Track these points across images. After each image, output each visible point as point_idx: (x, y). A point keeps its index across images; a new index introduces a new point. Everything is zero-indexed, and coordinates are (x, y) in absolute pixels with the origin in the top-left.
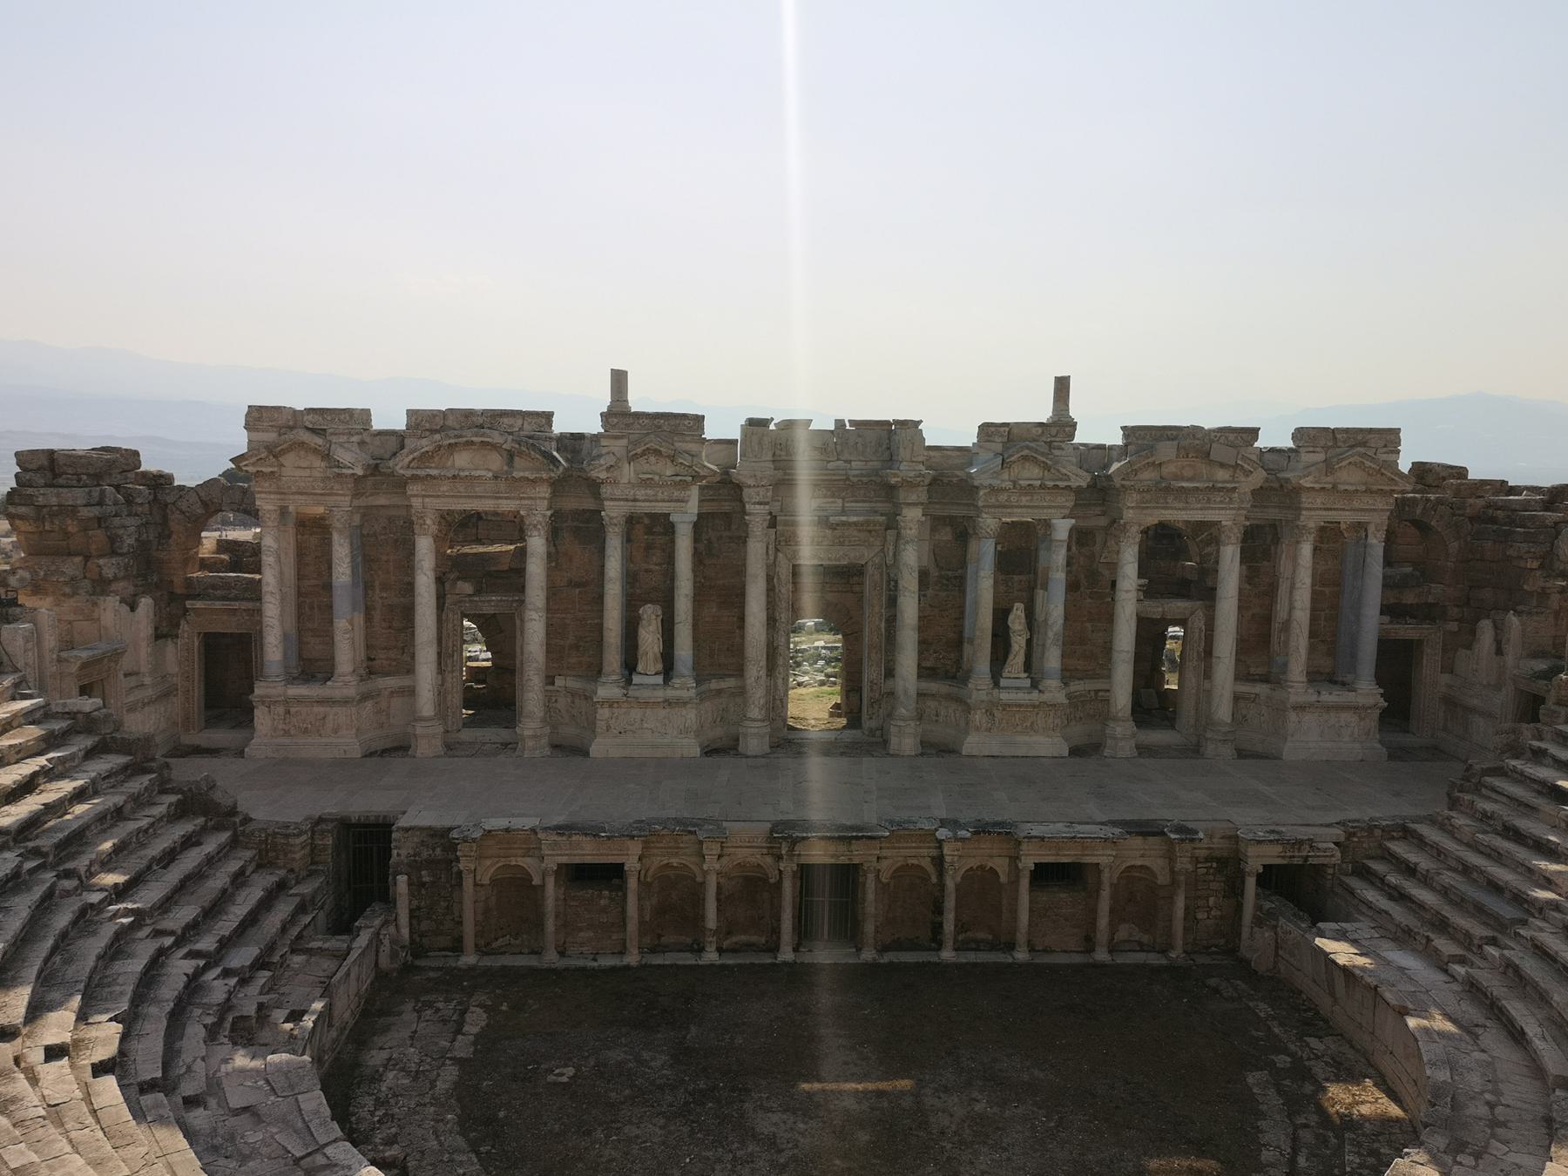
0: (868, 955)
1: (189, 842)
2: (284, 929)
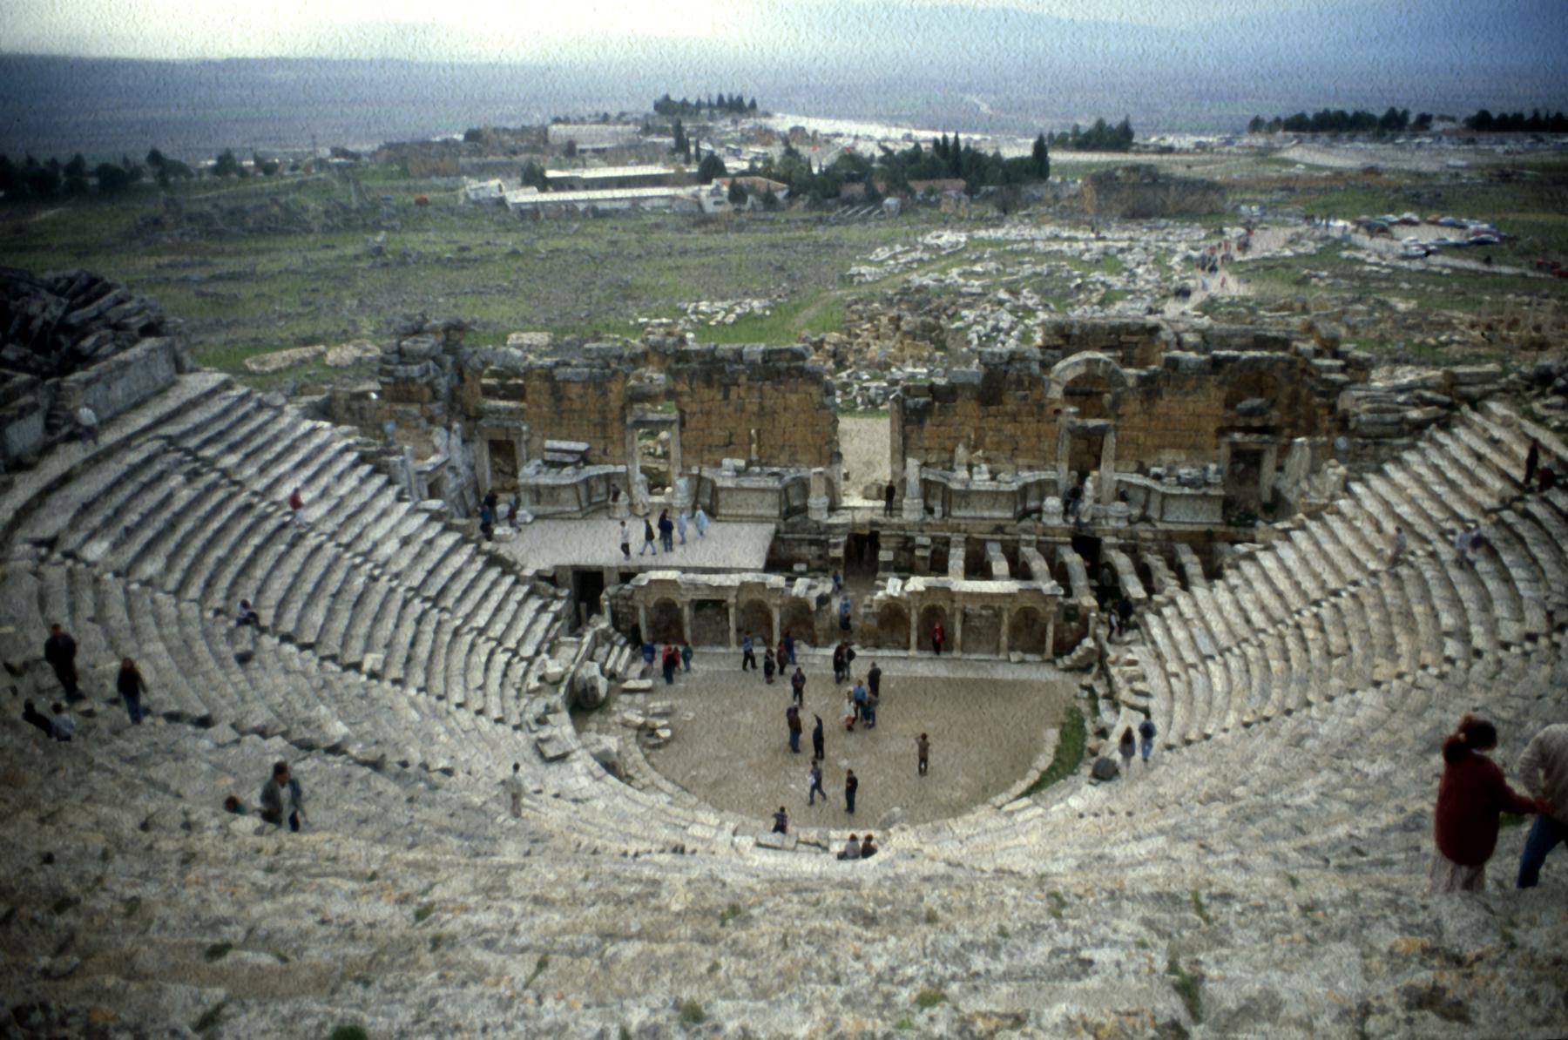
1: (495, 584)
2: (547, 631)
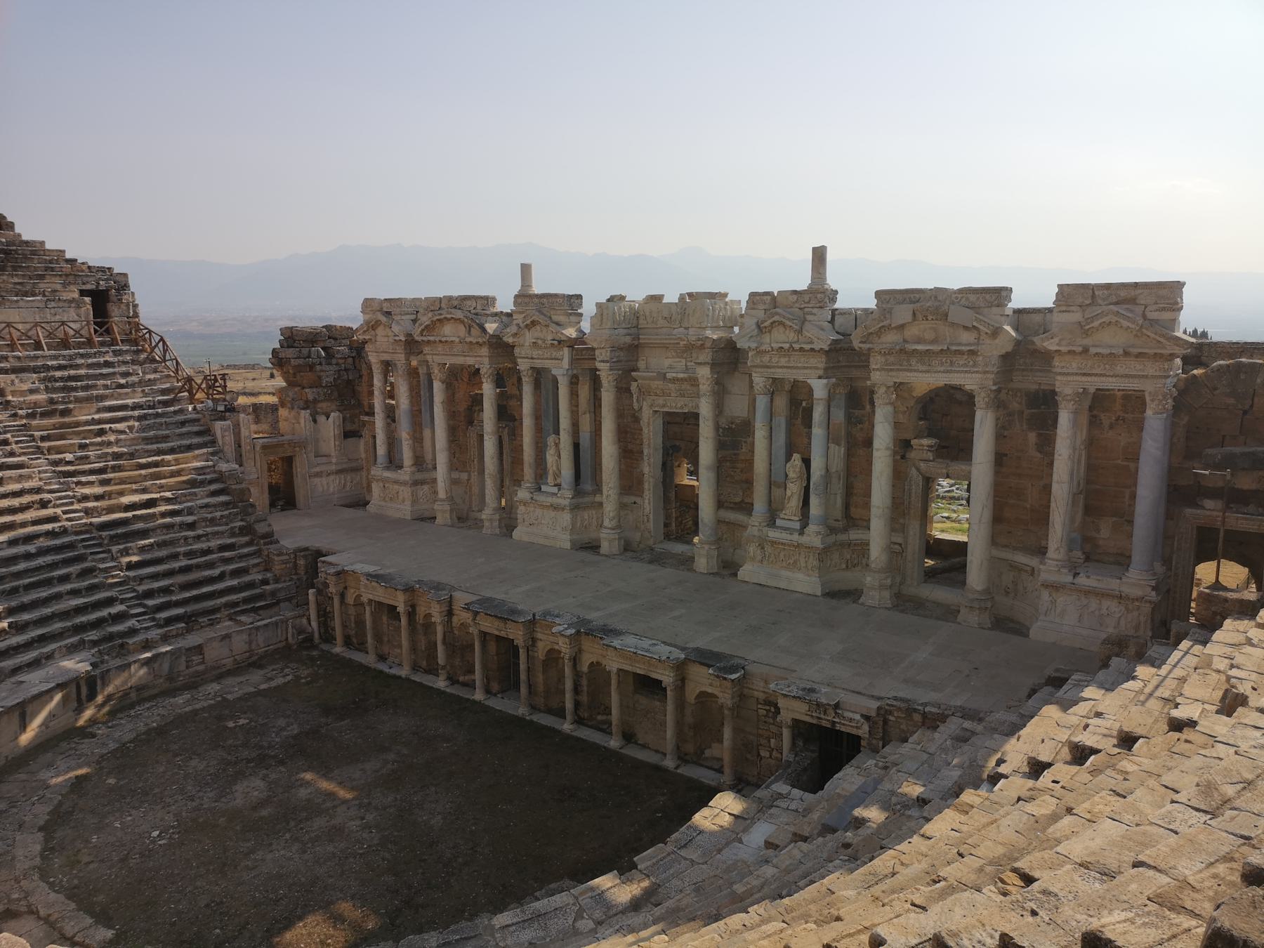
0: (522, 711)
